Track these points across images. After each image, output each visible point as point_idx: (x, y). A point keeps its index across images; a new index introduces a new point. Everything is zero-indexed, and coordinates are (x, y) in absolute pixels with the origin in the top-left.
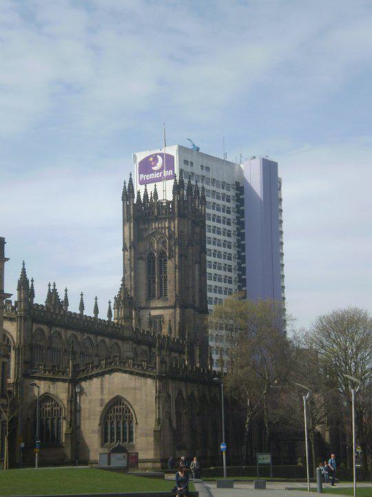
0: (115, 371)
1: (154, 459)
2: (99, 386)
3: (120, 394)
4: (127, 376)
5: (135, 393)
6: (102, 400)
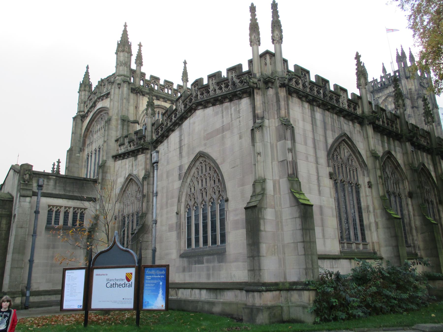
0: (195, 110)
1: (246, 284)
2: (178, 146)
3: (202, 149)
4: (210, 110)
5: (223, 138)
6: (180, 168)
